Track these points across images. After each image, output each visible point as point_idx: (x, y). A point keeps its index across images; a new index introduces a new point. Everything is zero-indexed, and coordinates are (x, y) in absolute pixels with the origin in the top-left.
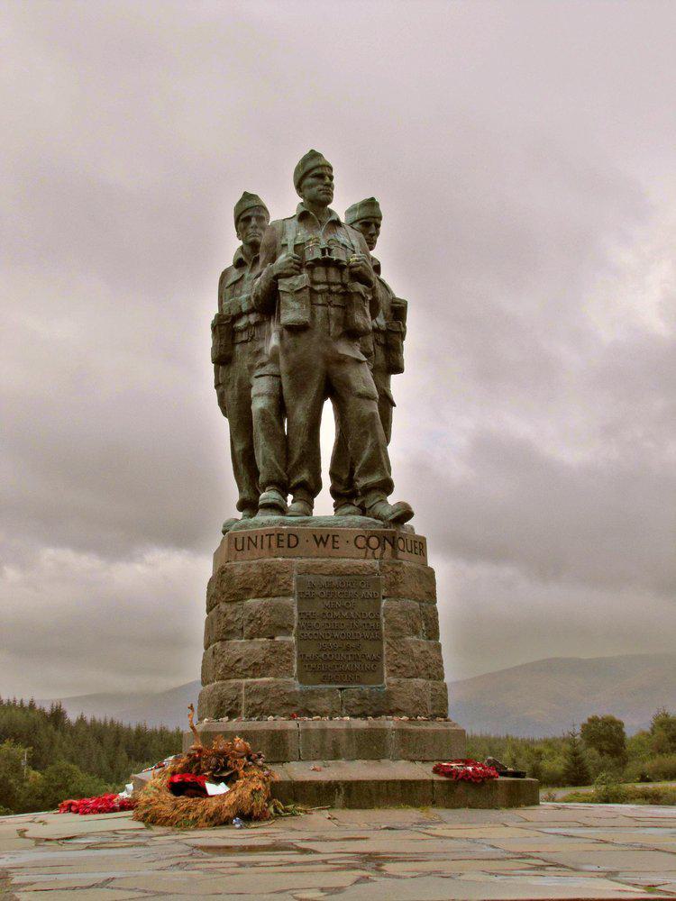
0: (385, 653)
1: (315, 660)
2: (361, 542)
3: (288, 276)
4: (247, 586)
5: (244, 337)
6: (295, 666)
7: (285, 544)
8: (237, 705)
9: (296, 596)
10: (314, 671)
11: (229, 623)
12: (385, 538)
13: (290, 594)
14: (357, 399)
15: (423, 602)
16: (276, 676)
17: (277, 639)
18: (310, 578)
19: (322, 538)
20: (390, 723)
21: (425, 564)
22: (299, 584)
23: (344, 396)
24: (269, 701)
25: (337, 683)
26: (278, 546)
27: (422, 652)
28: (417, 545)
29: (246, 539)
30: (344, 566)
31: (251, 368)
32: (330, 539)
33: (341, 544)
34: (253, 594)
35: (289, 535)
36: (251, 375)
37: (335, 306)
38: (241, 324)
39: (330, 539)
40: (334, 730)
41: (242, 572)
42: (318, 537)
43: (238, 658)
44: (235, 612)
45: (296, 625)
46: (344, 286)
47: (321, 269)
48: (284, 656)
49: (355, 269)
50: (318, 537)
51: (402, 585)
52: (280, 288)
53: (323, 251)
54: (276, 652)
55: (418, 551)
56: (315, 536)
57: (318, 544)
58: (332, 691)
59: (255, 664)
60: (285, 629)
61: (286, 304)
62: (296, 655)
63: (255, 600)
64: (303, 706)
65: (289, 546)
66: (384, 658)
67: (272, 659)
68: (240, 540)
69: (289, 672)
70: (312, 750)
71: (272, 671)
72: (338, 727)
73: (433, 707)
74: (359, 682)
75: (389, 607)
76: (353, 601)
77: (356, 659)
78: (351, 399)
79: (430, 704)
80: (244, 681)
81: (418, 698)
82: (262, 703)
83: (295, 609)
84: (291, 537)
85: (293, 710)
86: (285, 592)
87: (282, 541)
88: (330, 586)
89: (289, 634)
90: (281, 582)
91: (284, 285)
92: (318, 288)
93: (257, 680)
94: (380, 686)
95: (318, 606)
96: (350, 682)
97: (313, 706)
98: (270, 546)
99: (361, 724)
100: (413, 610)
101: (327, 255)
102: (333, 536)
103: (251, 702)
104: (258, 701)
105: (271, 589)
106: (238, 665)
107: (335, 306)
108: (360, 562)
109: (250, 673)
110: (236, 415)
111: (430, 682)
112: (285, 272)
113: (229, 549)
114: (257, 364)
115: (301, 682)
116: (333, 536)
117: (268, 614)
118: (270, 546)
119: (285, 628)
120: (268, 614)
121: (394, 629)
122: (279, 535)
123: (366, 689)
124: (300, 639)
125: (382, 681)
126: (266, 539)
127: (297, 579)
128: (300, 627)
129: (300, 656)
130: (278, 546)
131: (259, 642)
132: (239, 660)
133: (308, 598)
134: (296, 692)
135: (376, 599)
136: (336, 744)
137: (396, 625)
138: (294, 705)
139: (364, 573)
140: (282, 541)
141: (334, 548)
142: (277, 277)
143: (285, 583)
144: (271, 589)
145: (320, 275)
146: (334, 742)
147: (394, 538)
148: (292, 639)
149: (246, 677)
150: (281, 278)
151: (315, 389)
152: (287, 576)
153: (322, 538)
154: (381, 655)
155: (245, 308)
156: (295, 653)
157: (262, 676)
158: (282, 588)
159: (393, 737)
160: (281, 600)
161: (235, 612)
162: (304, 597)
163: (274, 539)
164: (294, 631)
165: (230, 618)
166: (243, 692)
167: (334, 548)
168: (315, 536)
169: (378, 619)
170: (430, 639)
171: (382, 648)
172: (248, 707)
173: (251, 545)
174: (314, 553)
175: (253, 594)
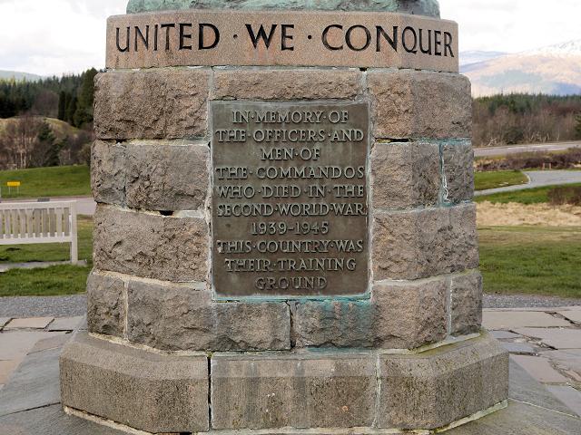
0: (372, 238)
1: (244, 254)
2: (336, 38)
4: (129, 118)
6: (209, 263)
7: (194, 42)
8: (117, 316)
9: (211, 140)
10: (243, 272)
11: (105, 176)
12: (379, 29)
13: (198, 137)
15: (446, 139)
16: (174, 278)
17: (180, 215)
18: (240, 107)
19: (262, 31)
20: (373, 363)
21: (454, 70)
22: (217, 120)
24: (162, 321)
25: (282, 292)
26: (181, 47)
27: (440, 231)
28: (441, 38)
29: (133, 31)
30: (300, 83)
32: (278, 30)
33: (298, 40)
34: (139, 134)
35: (201, 26)
39: (278, 30)
40: (273, 381)
41: (122, 90)
42: (256, 31)
43: (118, 238)
44: (114, 159)
45: (210, 191)
48: (189, 244)
50: (256, 31)
51: (406, 117)
54: (174, 236)
55: (441, 48)
56: (249, 27)
57: (254, 41)
58: (271, 305)
59: (141, 254)
60: (194, 199)
62: (210, 244)
63: (144, 143)
64: (223, 332)
65: (201, 47)
66: (371, 245)
67: (168, 251)
68: (123, 32)
69: (195, 272)
70: (232, 413)
71: (167, 270)
72: (279, 374)
73: (456, 319)
74: (325, 291)
75: (384, 157)
76: (317, 146)
77: (317, 249)
79: (450, 315)
80: (126, 278)
81: (427, 314)
82: (150, 324)
83: (209, 163)
84: (206, 29)
85: (205, 339)
86: (190, 132)
87: (189, 36)
88: (273, 121)
89: (199, 205)
90: (183, 114)
93: (146, 281)
94: (360, 295)
95: (255, 152)
96: (307, 290)
97: (239, 332)
98: (167, 48)
99: (322, 365)
100: (427, 159)
102: (284, 27)
103: (136, 317)
104: (146, 322)
105: (165, 127)
106: (119, 250)
108: (331, 75)
109: (135, 267)
111: (451, 280)
113: (108, 48)
115: (218, 291)
116: (284, 27)
117: (160, 170)
118: (167, 48)
119: (193, 196)
120: (160, 170)
121: (392, 196)
122: (182, 26)
123: (330, 301)
124: (215, 216)
125: (364, 288)
126: (162, 31)
127: (214, 109)
128: (214, 197)
129: (216, 245)
130: (181, 47)
131: (148, 217)
132: (119, 243)
133: (232, 141)
134: (207, 309)
135: (360, 144)
136: (276, 403)
137: (397, 189)
138: (206, 331)
139: (336, 94)
140: (189, 36)
141: (283, 48)
143: (191, 115)
144: (165, 127)
146: (273, 399)
147: (395, 28)
148: (205, 215)
149: (130, 272)
152: (195, 102)
153: (262, 31)
154: (364, 243)
156: (209, 240)
157: (153, 276)
158: (185, 124)
159: (378, 390)
160: (182, 144)
161: (114, 159)
162: (221, 142)
163: (174, 32)
164: (208, 202)
165: (106, 167)
166: (125, 297)
167: (283, 48)
168: (249, 27)
169: (364, 179)
170: (456, 202)
171: (366, 231)
172: (133, 325)
173: (140, 42)
174: (248, 59)
175: (139, 134)
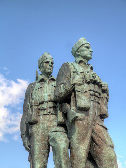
3: (81, 85)
5: (46, 112)
14: (109, 148)
23: (101, 145)
31: (49, 127)
36: (48, 130)
37: (97, 102)
38: (45, 106)
46: (100, 94)
47: (93, 85)
49: (103, 88)
52: (76, 89)
53: (93, 77)
61: (80, 97)
78: (105, 147)
91: (77, 88)
92: (92, 93)
101: (96, 79)
107: (97, 102)
110: (38, 149)
112: (79, 82)
114: (52, 125)
142: (74, 85)
145: (91, 87)
150: (77, 85)
151: (89, 140)
155: (47, 99)
